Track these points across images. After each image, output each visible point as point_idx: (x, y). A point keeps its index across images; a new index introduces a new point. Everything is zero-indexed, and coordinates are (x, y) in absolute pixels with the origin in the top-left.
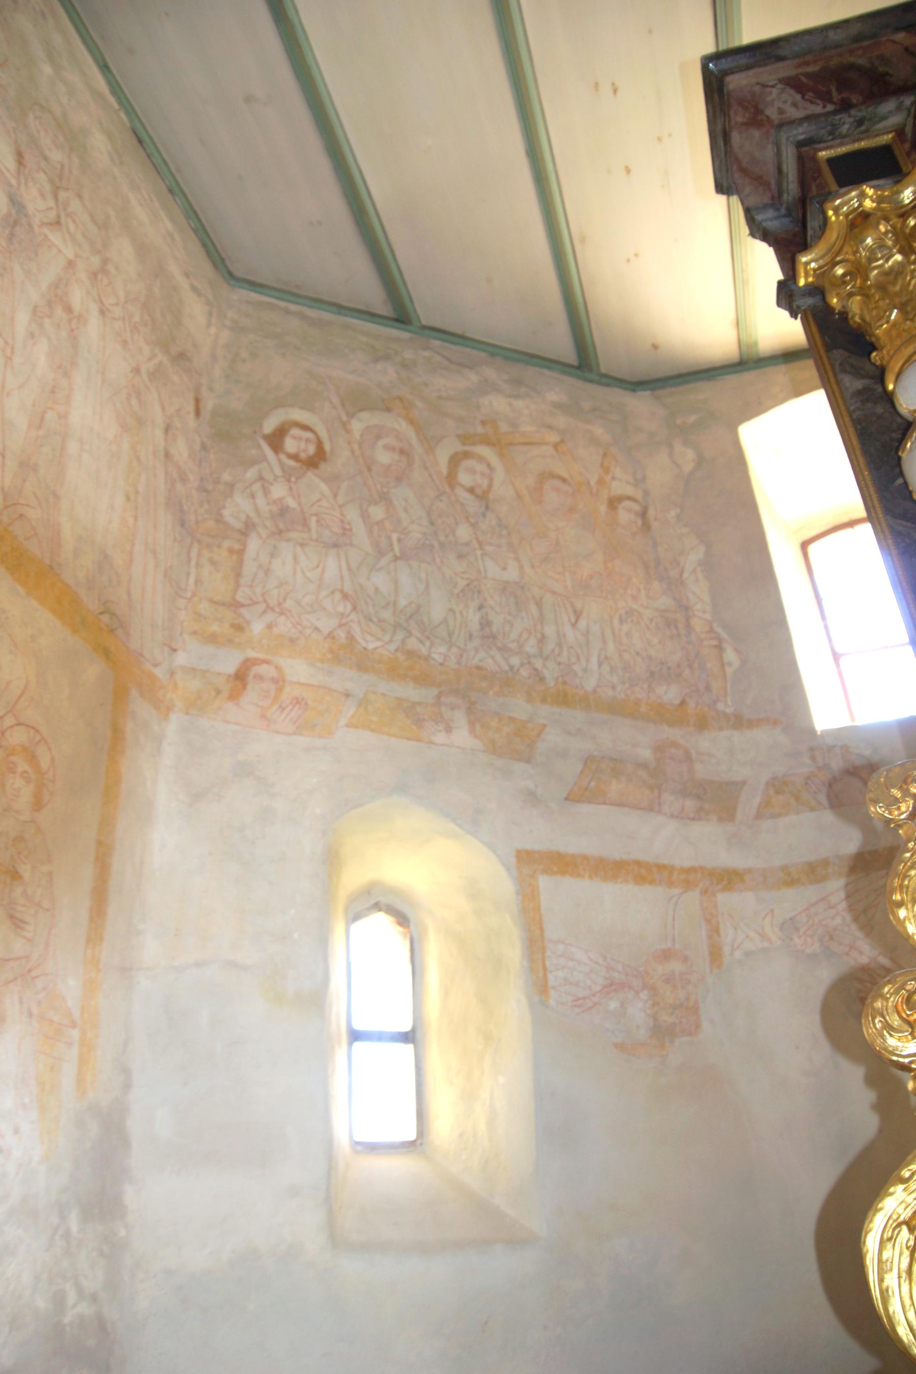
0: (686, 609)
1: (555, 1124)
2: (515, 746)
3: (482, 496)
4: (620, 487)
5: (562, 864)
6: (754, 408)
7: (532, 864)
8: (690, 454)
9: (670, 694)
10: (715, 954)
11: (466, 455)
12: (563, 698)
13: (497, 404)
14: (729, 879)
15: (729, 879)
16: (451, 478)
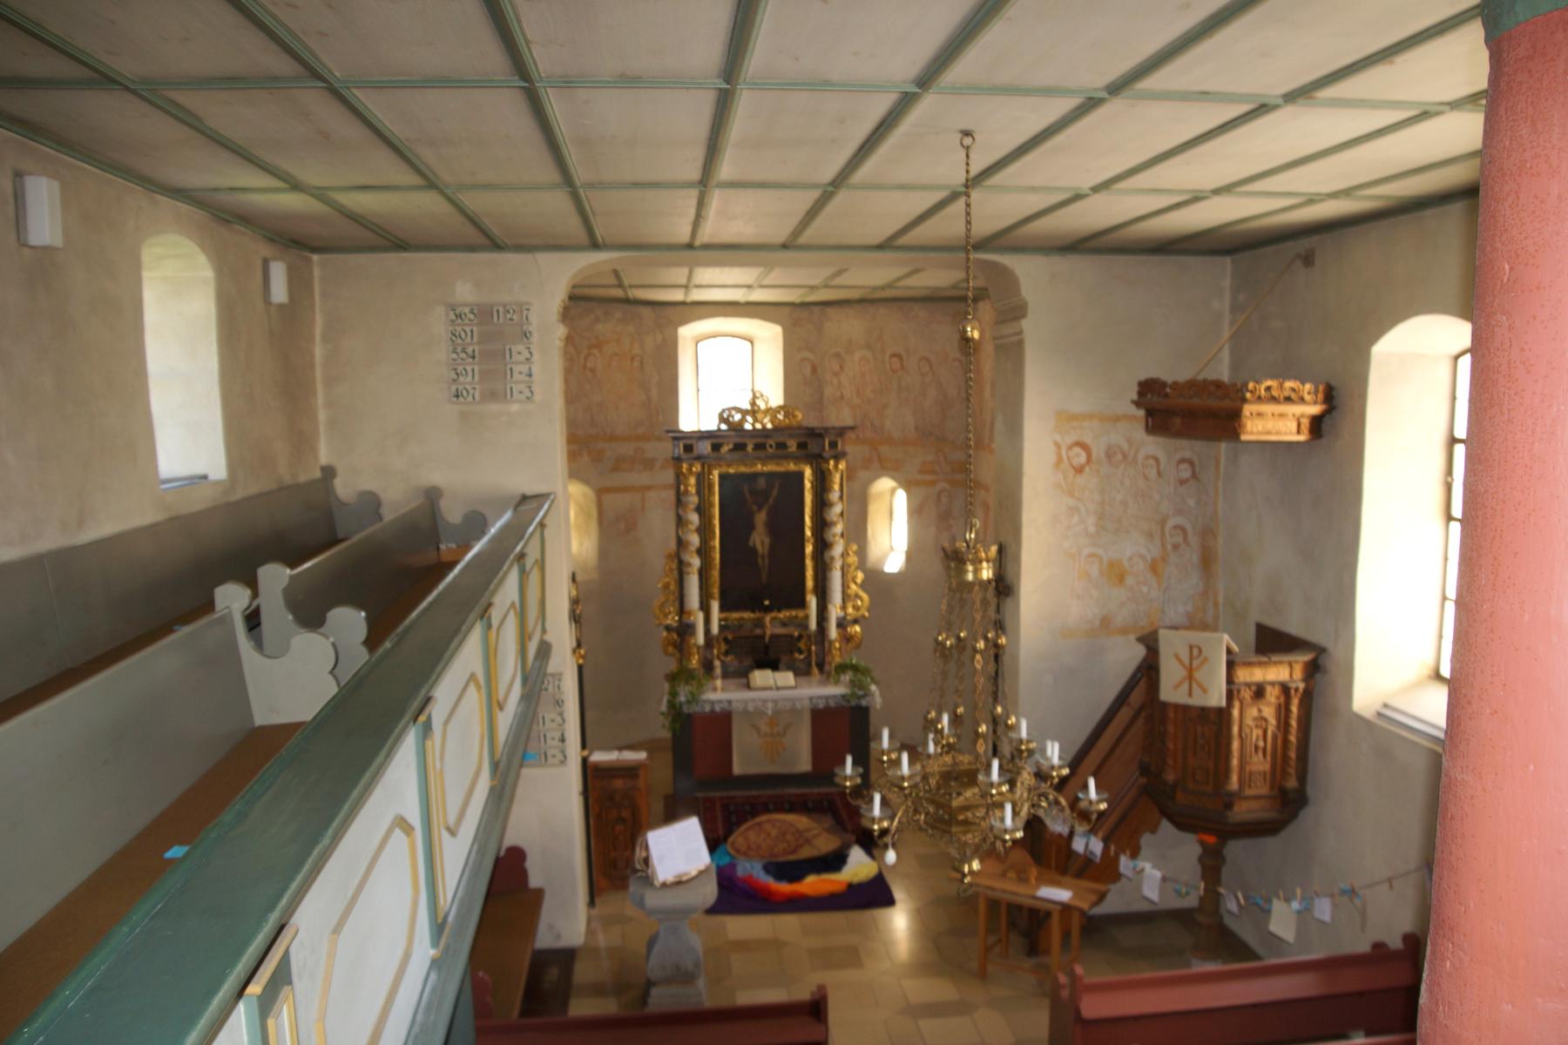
0: (649, 400)
1: (603, 553)
2: (597, 458)
3: (593, 370)
4: (636, 351)
5: (607, 490)
6: (685, 321)
7: (600, 492)
8: (659, 338)
9: (641, 431)
10: (643, 508)
11: (589, 354)
12: (613, 438)
13: (600, 327)
14: (649, 488)
15: (649, 488)
16: (585, 367)
